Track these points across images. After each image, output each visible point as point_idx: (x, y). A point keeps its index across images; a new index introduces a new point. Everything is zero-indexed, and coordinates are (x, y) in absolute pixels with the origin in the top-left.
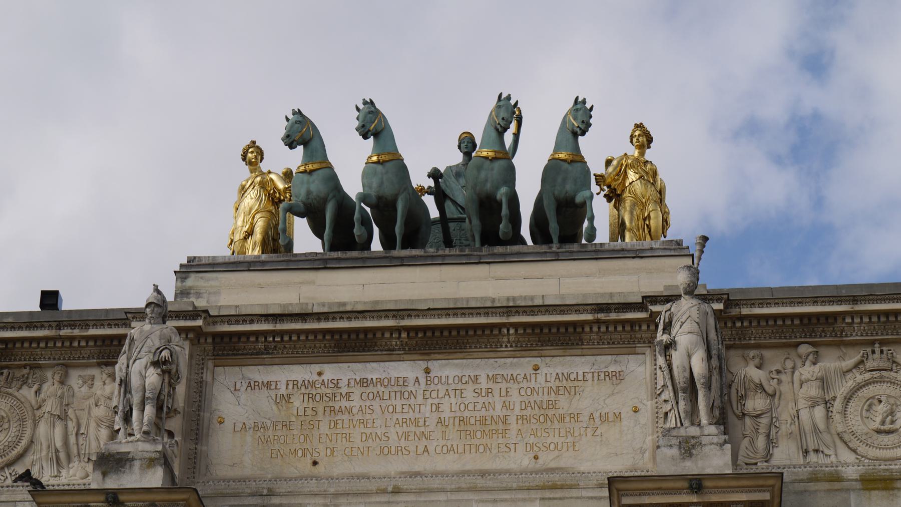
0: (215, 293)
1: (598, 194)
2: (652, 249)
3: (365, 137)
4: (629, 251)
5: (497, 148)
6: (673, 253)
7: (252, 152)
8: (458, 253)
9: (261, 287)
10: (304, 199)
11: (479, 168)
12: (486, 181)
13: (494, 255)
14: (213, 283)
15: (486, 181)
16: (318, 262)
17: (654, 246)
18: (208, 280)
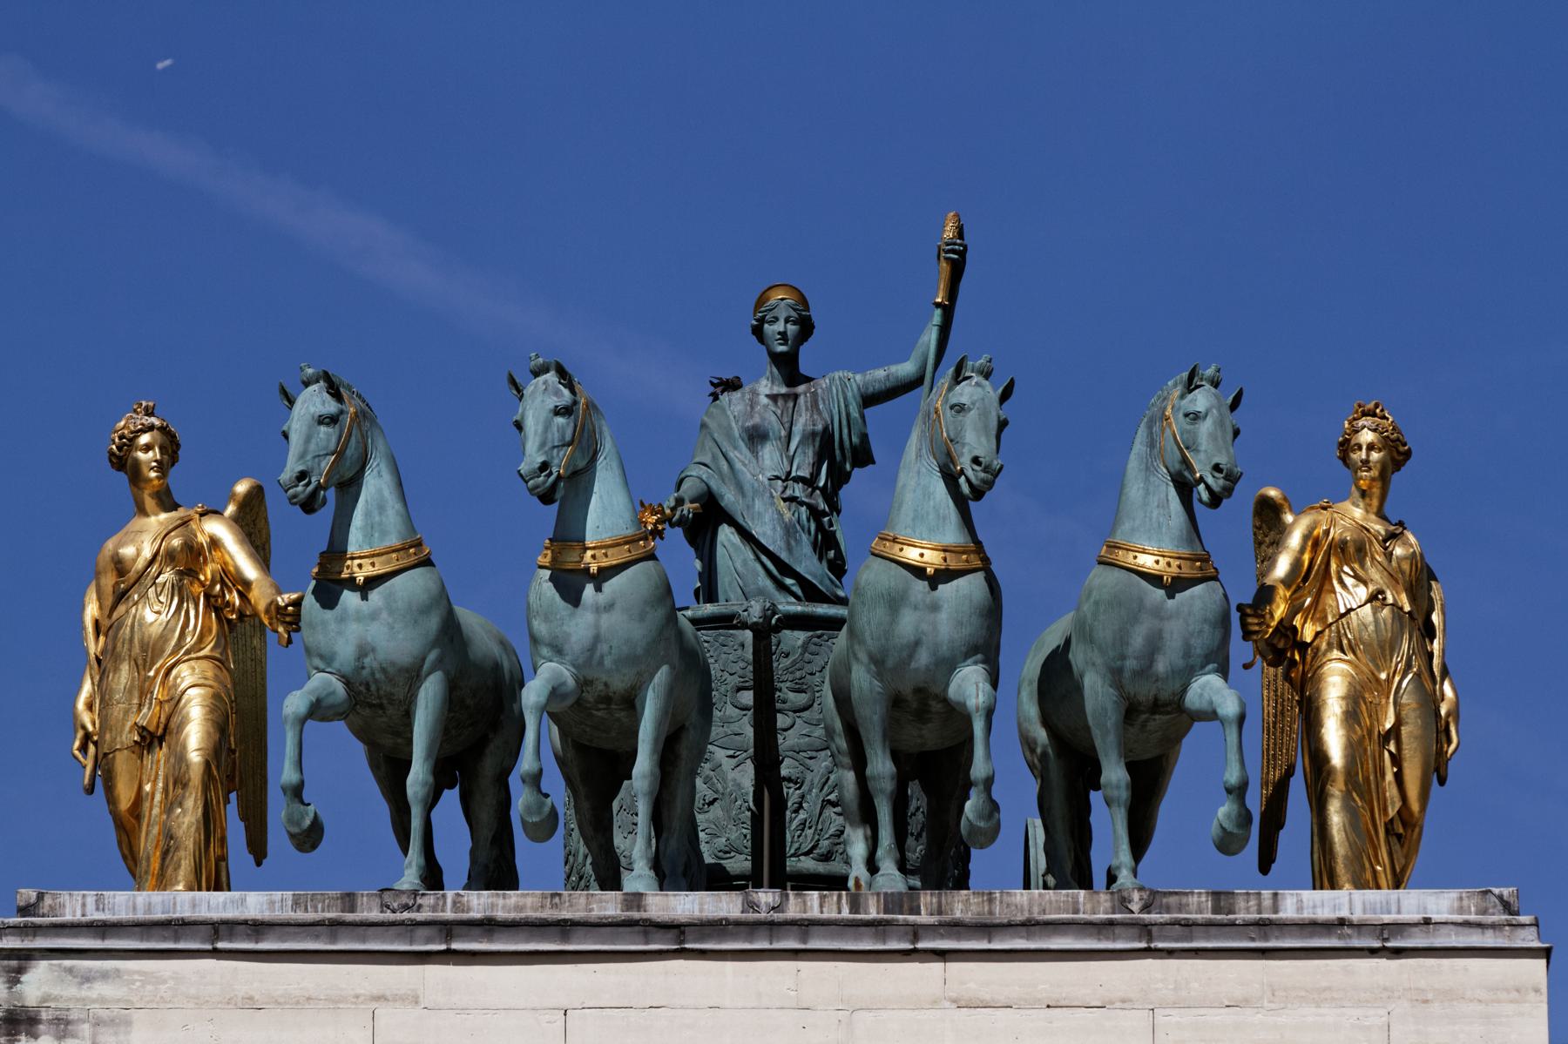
0: (112, 1022)
1: (1247, 666)
2: (1427, 922)
4: (1360, 927)
5: (952, 534)
6: (1489, 940)
7: (148, 448)
8: (846, 913)
9: (252, 1005)
10: (347, 669)
11: (895, 603)
12: (917, 643)
13: (956, 927)
14: (100, 989)
15: (917, 643)
16: (422, 932)
17: (1436, 917)
18: (87, 979)
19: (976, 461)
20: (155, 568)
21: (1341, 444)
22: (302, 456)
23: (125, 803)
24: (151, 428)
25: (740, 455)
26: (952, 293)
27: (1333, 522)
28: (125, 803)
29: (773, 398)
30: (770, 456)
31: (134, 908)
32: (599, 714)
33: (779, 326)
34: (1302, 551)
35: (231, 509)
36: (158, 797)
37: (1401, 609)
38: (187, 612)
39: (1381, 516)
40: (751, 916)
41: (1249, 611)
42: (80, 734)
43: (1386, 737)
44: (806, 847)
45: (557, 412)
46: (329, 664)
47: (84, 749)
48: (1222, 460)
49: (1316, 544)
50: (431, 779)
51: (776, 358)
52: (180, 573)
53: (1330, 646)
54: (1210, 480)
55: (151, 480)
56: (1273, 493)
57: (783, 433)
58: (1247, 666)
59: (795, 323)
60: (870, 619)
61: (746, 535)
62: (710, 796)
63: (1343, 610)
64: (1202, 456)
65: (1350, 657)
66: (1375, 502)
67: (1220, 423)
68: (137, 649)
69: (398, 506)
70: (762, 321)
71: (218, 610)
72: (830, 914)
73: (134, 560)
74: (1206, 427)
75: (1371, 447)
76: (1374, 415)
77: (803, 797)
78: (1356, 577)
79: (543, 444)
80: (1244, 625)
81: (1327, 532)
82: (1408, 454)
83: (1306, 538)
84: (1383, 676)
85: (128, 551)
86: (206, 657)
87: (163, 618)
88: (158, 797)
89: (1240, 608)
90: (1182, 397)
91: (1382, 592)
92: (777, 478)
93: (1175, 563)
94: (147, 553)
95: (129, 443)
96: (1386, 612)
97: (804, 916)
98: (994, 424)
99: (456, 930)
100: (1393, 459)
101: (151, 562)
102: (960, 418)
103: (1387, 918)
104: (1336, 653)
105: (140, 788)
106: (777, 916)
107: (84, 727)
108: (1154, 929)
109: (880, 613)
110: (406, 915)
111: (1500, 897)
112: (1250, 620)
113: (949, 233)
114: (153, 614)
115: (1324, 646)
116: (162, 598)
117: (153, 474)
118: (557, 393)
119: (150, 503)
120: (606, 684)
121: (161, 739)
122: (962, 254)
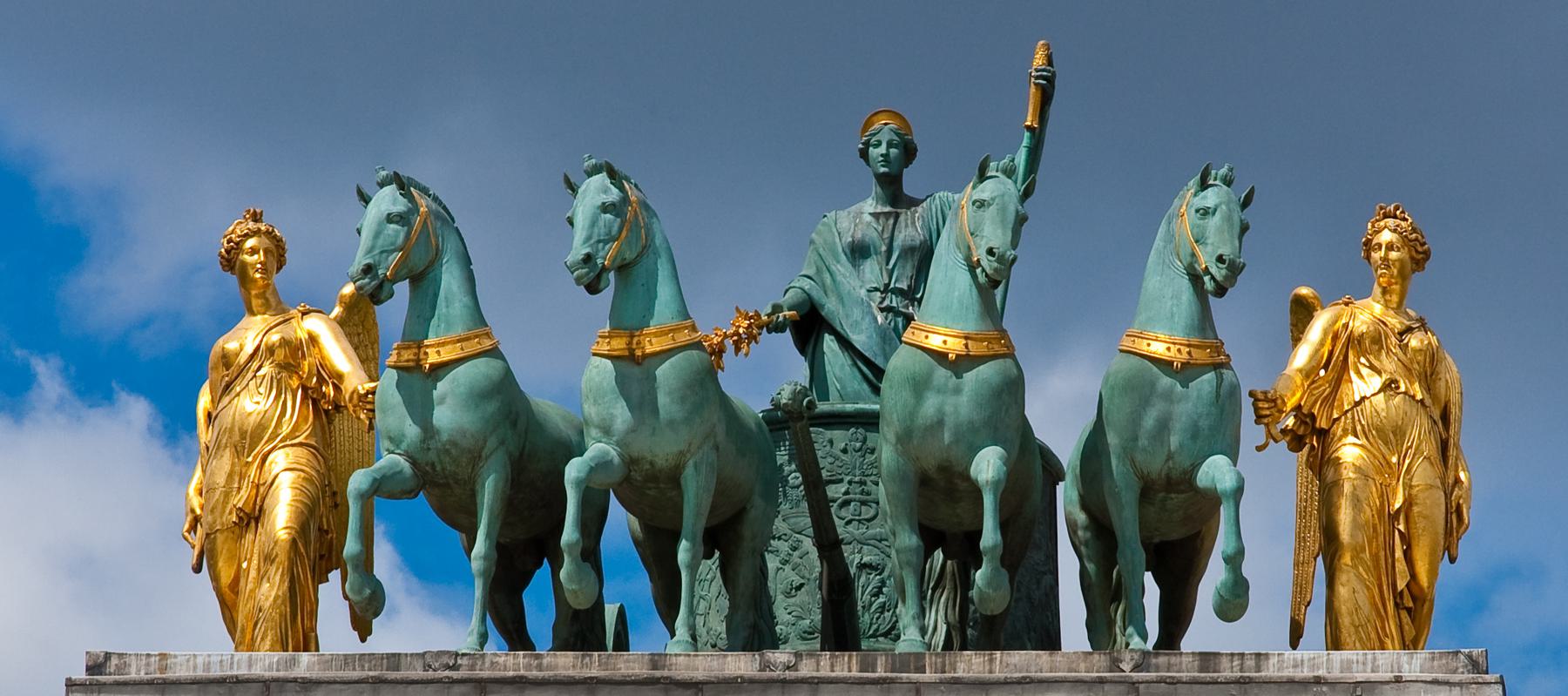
1: (1259, 449)
2: (1398, 680)
3: (593, 288)
5: (972, 325)
7: (254, 251)
8: (855, 673)
11: (920, 386)
12: (940, 423)
17: (1406, 675)
19: (990, 252)
20: (255, 365)
21: (1366, 244)
22: (370, 251)
23: (226, 579)
24: (257, 233)
25: (843, 268)
26: (1043, 115)
27: (1353, 316)
28: (226, 579)
29: (876, 215)
30: (872, 271)
31: (195, 668)
32: (651, 493)
33: (883, 149)
34: (1322, 344)
35: (337, 311)
36: (253, 573)
37: (1413, 397)
38: (285, 403)
39: (1399, 309)
40: (767, 674)
41: (1261, 396)
42: (190, 518)
43: (1394, 517)
44: (883, 629)
45: (605, 208)
46: (398, 447)
47: (193, 528)
48: (1226, 251)
49: (1336, 337)
50: (495, 555)
51: (881, 179)
52: (279, 365)
53: (1345, 433)
54: (1213, 270)
55: (255, 280)
56: (1304, 291)
57: (884, 248)
58: (1259, 449)
59: (896, 147)
60: (892, 401)
61: (845, 343)
62: (797, 581)
63: (1357, 399)
64: (1209, 248)
65: (1363, 441)
66: (1395, 298)
67: (1228, 219)
68: (237, 437)
69: (466, 300)
70: (867, 144)
71: (315, 402)
72: (839, 673)
73: (237, 355)
74: (1214, 222)
75: (1390, 247)
76: (1395, 217)
77: (883, 583)
78: (1372, 367)
79: (588, 238)
80: (1256, 409)
81: (1346, 326)
82: (1427, 254)
83: (1325, 333)
84: (1394, 459)
85: (232, 346)
86: (301, 444)
87: (262, 408)
88: (253, 573)
89: (1251, 394)
90: (1195, 195)
91: (1395, 381)
92: (876, 289)
93: (1185, 350)
94: (249, 349)
95: (236, 248)
96: (1398, 399)
97: (815, 674)
98: (1011, 217)
99: (490, 687)
100: (1412, 258)
101: (252, 356)
102: (980, 212)
103: (1360, 677)
104: (1351, 439)
105: (239, 566)
106: (789, 674)
107: (193, 511)
108: (1142, 687)
109: (906, 395)
110: (447, 673)
111: (1469, 656)
112: (1260, 405)
113: (1039, 60)
114: (252, 403)
115: (1339, 432)
116: (262, 390)
117: (258, 275)
118: (606, 191)
119: (255, 303)
120: (651, 463)
121: (257, 520)
122: (1050, 80)
